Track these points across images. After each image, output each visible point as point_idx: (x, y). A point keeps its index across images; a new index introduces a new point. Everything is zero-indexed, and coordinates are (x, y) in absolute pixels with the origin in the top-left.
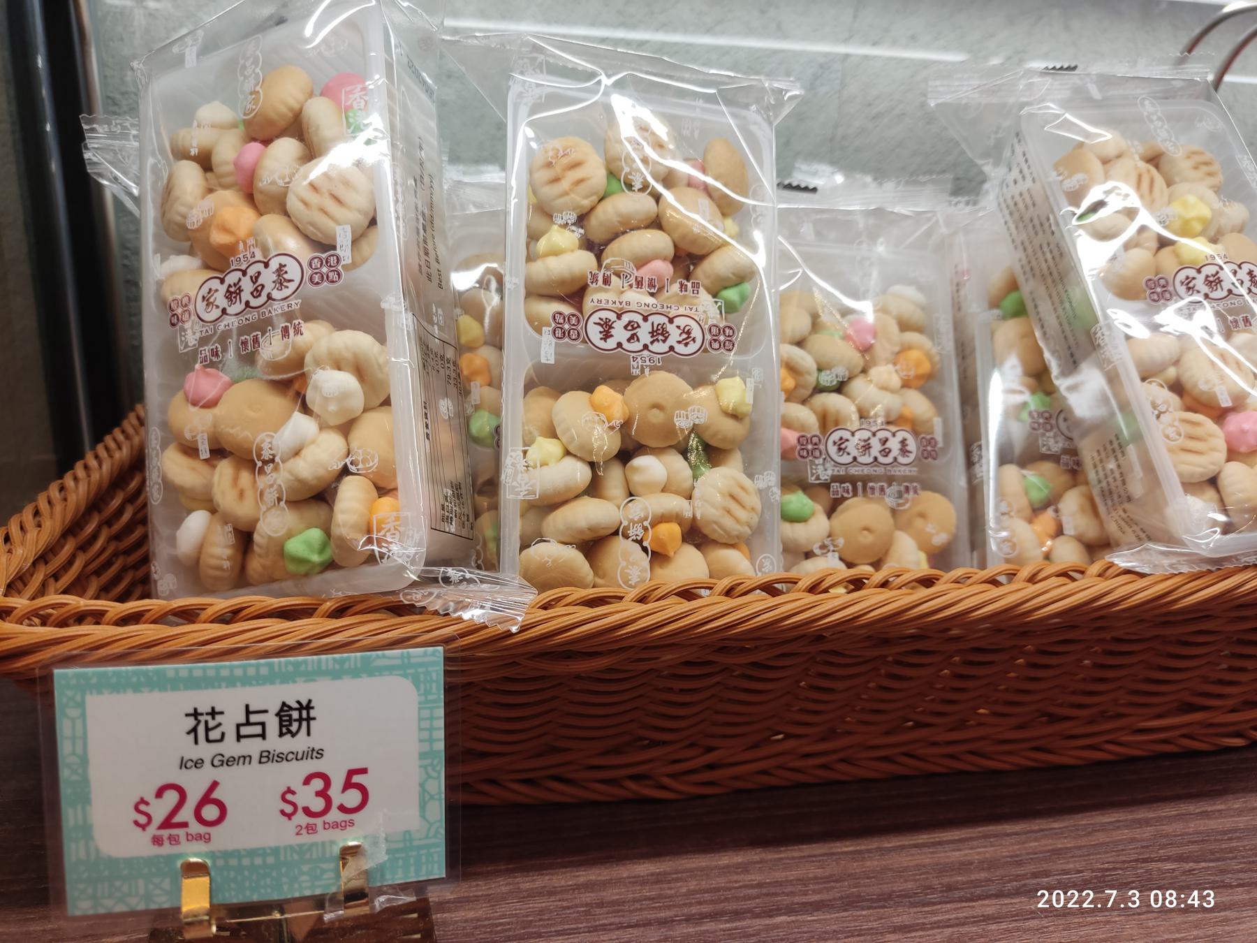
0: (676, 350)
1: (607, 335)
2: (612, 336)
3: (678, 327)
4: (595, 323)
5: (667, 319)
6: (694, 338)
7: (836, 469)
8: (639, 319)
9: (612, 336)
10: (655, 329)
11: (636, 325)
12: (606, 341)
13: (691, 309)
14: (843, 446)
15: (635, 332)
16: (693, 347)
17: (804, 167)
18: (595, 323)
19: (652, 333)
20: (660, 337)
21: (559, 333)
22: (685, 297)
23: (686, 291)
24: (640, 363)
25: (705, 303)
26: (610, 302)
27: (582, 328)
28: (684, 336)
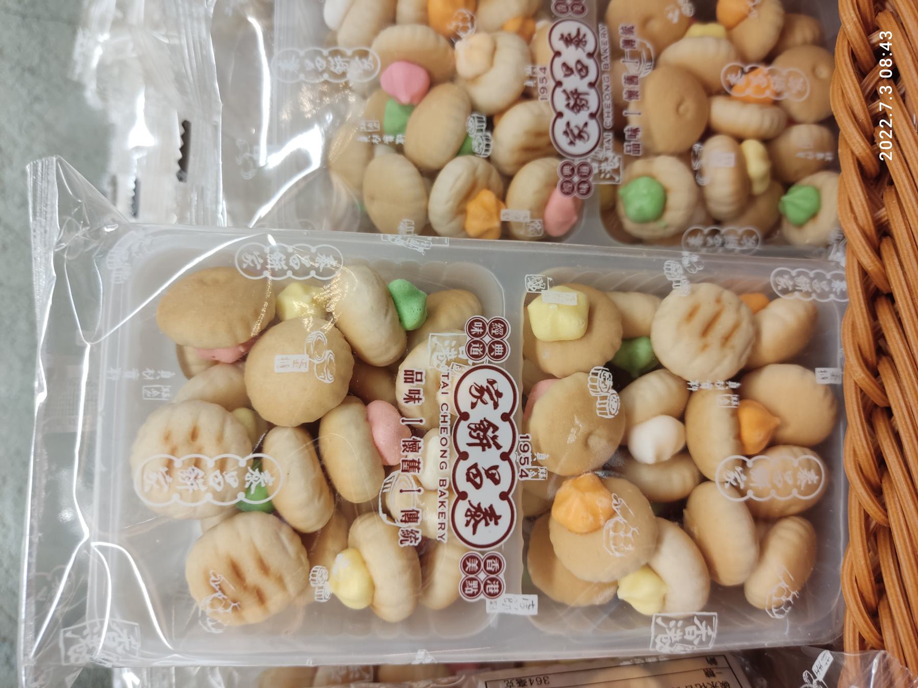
0: (508, 411)
1: (491, 515)
2: (491, 507)
3: (473, 405)
4: (474, 533)
5: (462, 422)
6: (488, 382)
7: (606, 145)
8: (464, 466)
9: (491, 507)
10: (477, 441)
11: (474, 471)
12: (500, 517)
13: (446, 385)
14: (576, 132)
15: (483, 472)
16: (503, 385)
17: (78, 70)
18: (474, 533)
19: (484, 446)
20: (490, 433)
21: (492, 588)
22: (426, 392)
23: (418, 392)
24: (530, 466)
25: (436, 363)
26: (442, 509)
27: (483, 553)
28: (486, 397)
